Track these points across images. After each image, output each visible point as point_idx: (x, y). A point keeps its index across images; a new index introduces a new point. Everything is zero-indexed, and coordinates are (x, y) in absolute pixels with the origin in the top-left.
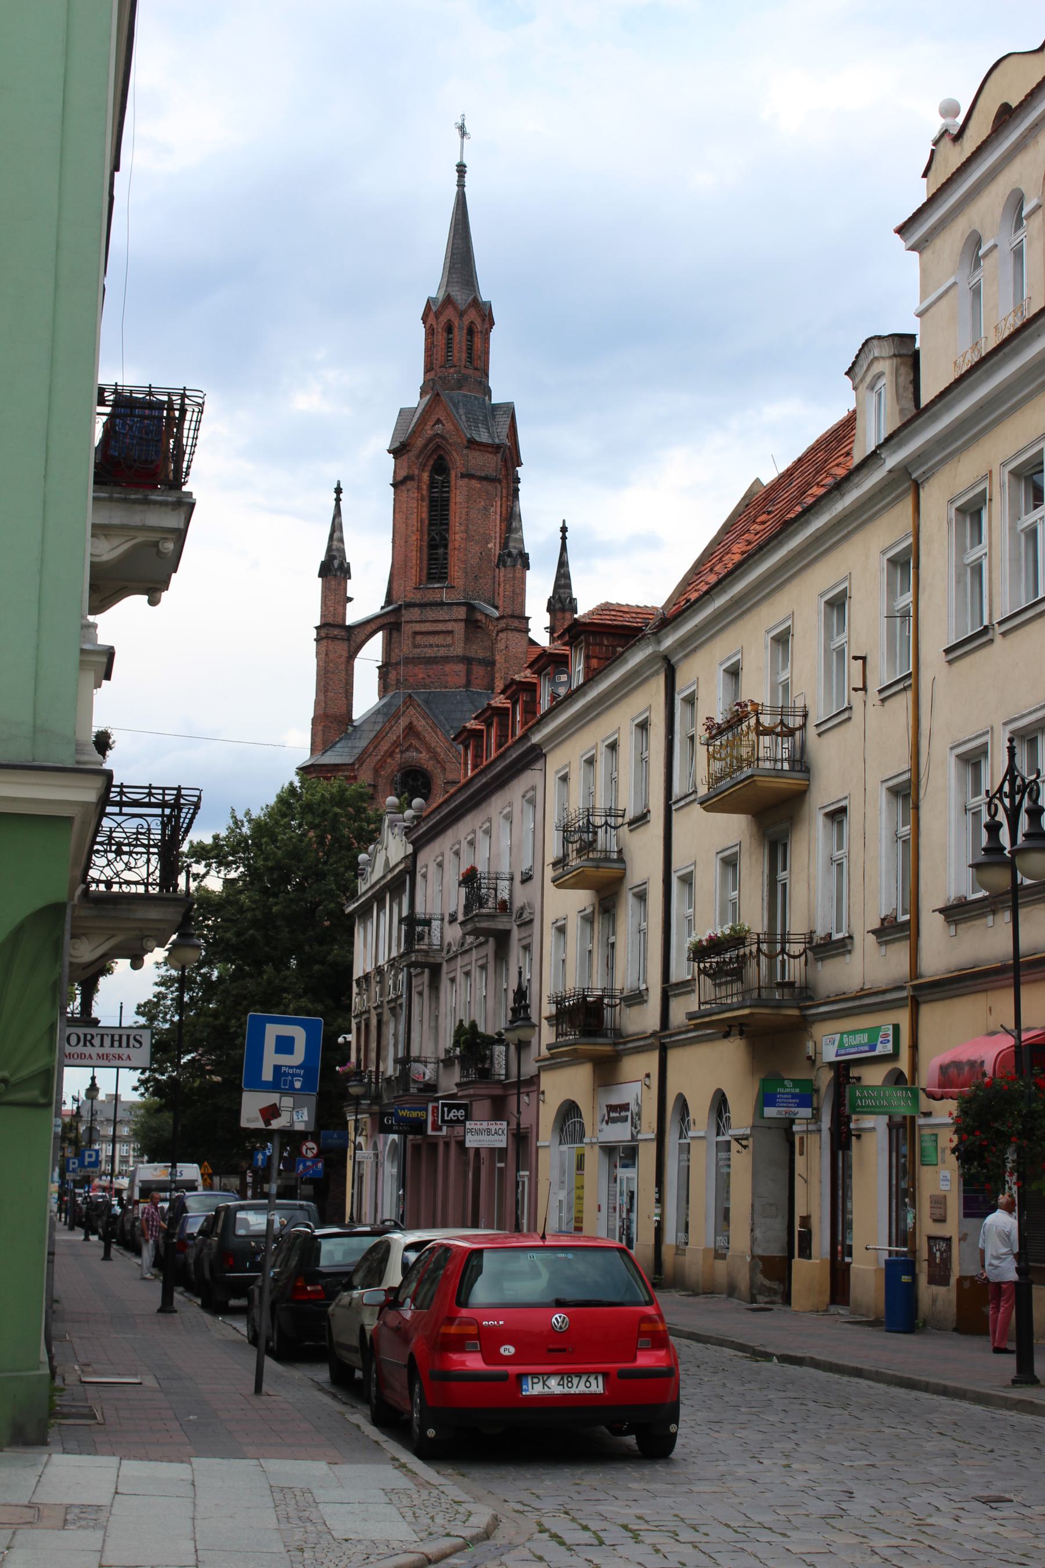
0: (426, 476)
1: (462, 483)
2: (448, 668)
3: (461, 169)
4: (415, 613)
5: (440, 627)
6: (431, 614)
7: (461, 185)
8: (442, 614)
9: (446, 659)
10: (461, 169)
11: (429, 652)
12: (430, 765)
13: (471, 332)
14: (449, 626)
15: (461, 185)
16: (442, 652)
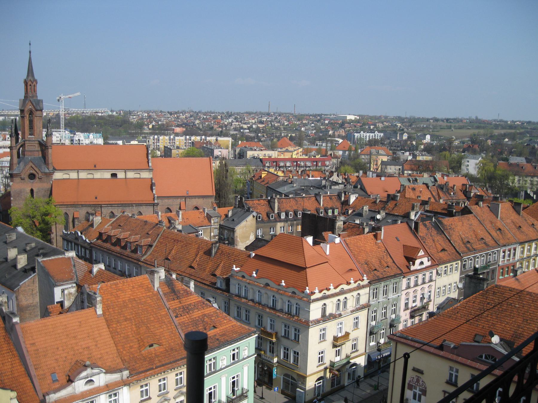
0: (28, 116)
1: (35, 118)
2: (35, 152)
3: (30, 52)
4: (27, 142)
5: (32, 145)
6: (31, 142)
7: (30, 55)
8: (33, 142)
9: (34, 151)
10: (30, 52)
11: (31, 149)
12: (35, 173)
13: (34, 86)
14: (34, 145)
15: (30, 55)
16: (34, 149)
